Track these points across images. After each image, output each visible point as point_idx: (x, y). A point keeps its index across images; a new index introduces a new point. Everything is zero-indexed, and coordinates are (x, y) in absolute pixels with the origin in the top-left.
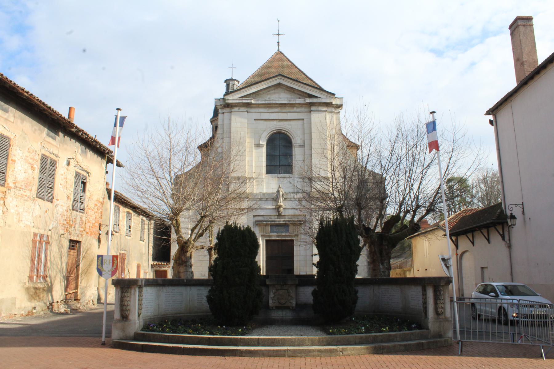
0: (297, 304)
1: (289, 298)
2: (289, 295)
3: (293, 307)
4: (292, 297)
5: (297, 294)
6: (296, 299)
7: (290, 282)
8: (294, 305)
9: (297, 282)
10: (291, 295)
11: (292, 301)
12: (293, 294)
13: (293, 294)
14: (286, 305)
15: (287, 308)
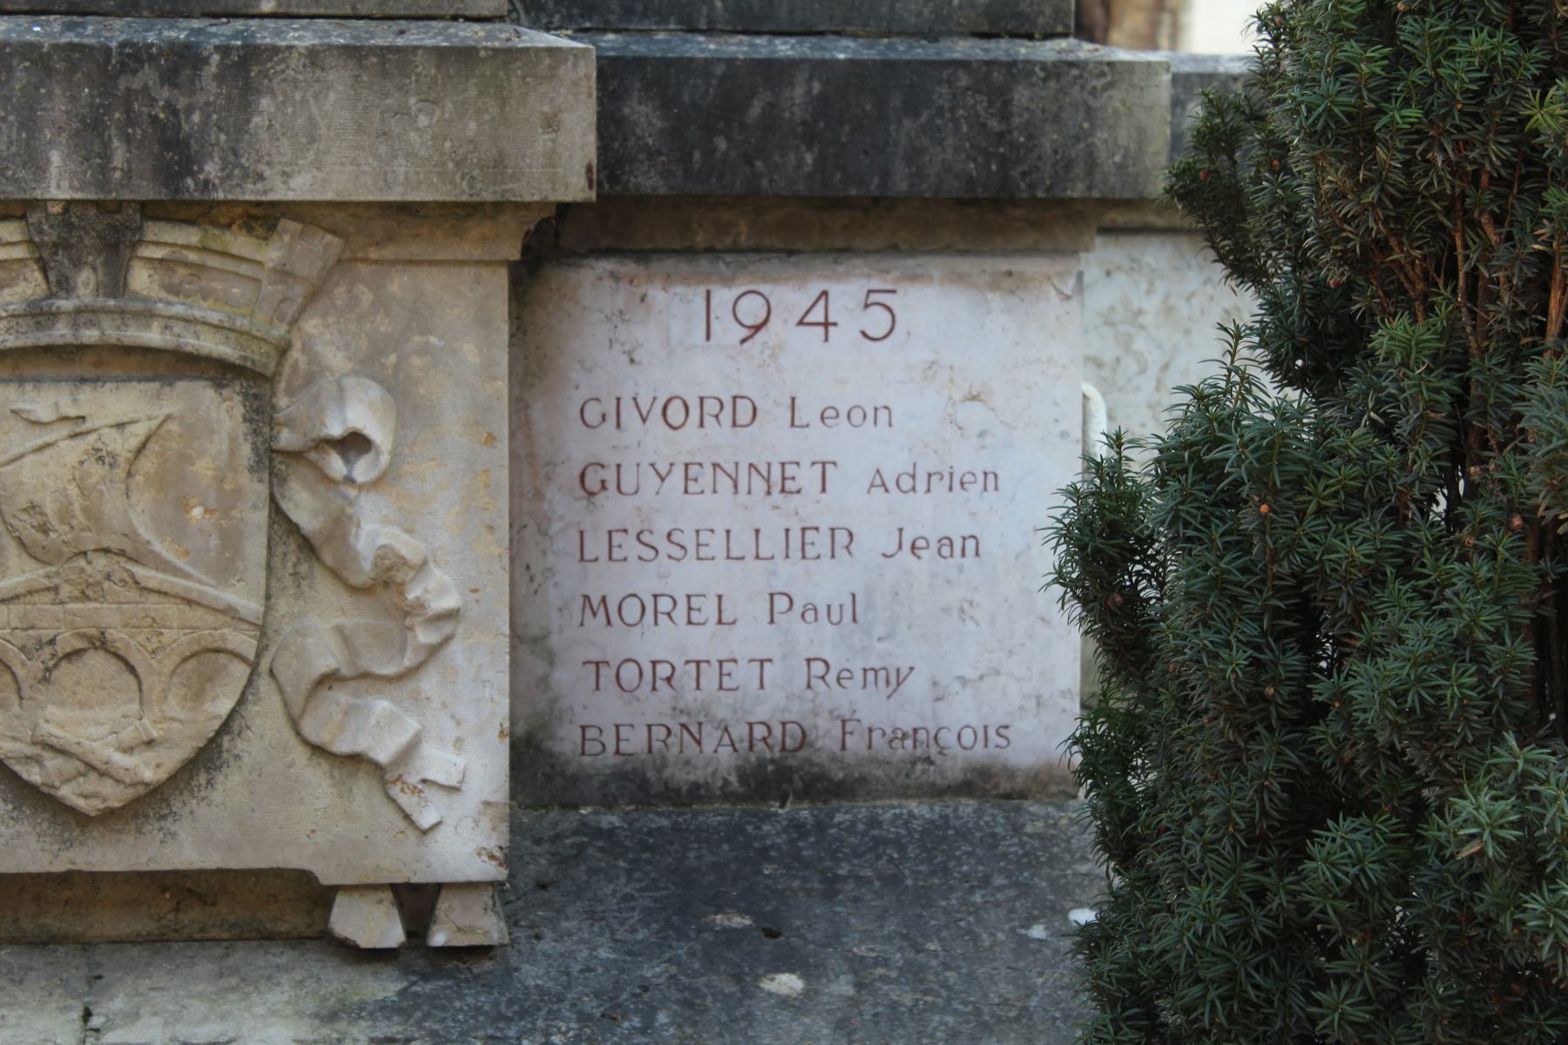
0: (533, 763)
1: (321, 628)
2: (302, 549)
3: (417, 901)
4: (384, 586)
5: (543, 494)
6: (529, 644)
7: (318, 145)
8: (461, 834)
9: (559, 153)
10: (375, 530)
11: (379, 727)
12: (430, 520)
13: (430, 520)
14: (187, 845)
15: (266, 915)
